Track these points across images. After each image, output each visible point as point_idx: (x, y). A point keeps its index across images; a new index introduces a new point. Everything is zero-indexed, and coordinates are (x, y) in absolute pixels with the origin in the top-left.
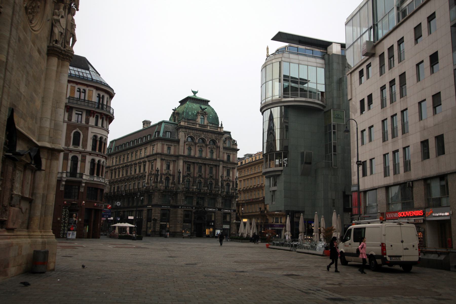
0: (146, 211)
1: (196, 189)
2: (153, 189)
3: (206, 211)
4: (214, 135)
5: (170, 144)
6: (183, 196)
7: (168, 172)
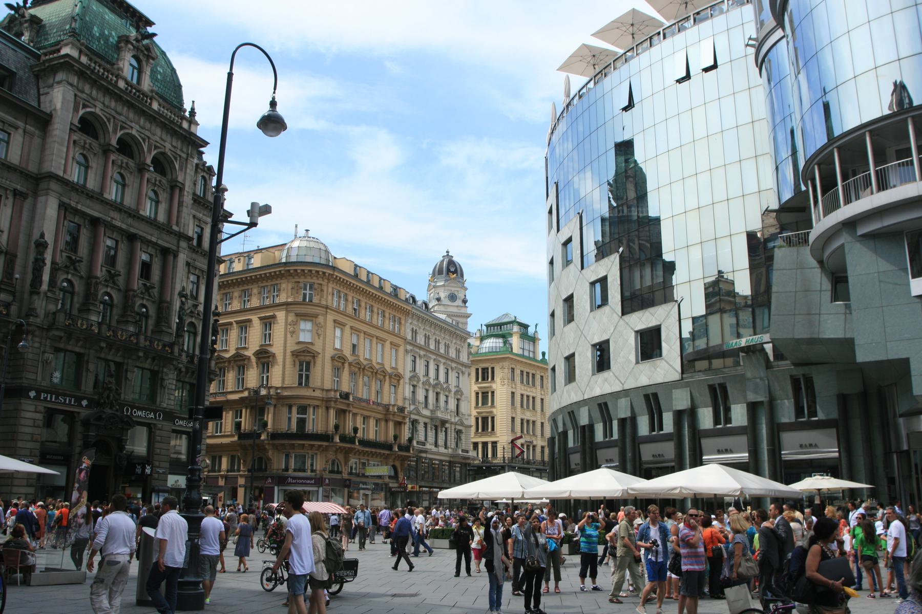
4: (168, 138)
6: (47, 349)
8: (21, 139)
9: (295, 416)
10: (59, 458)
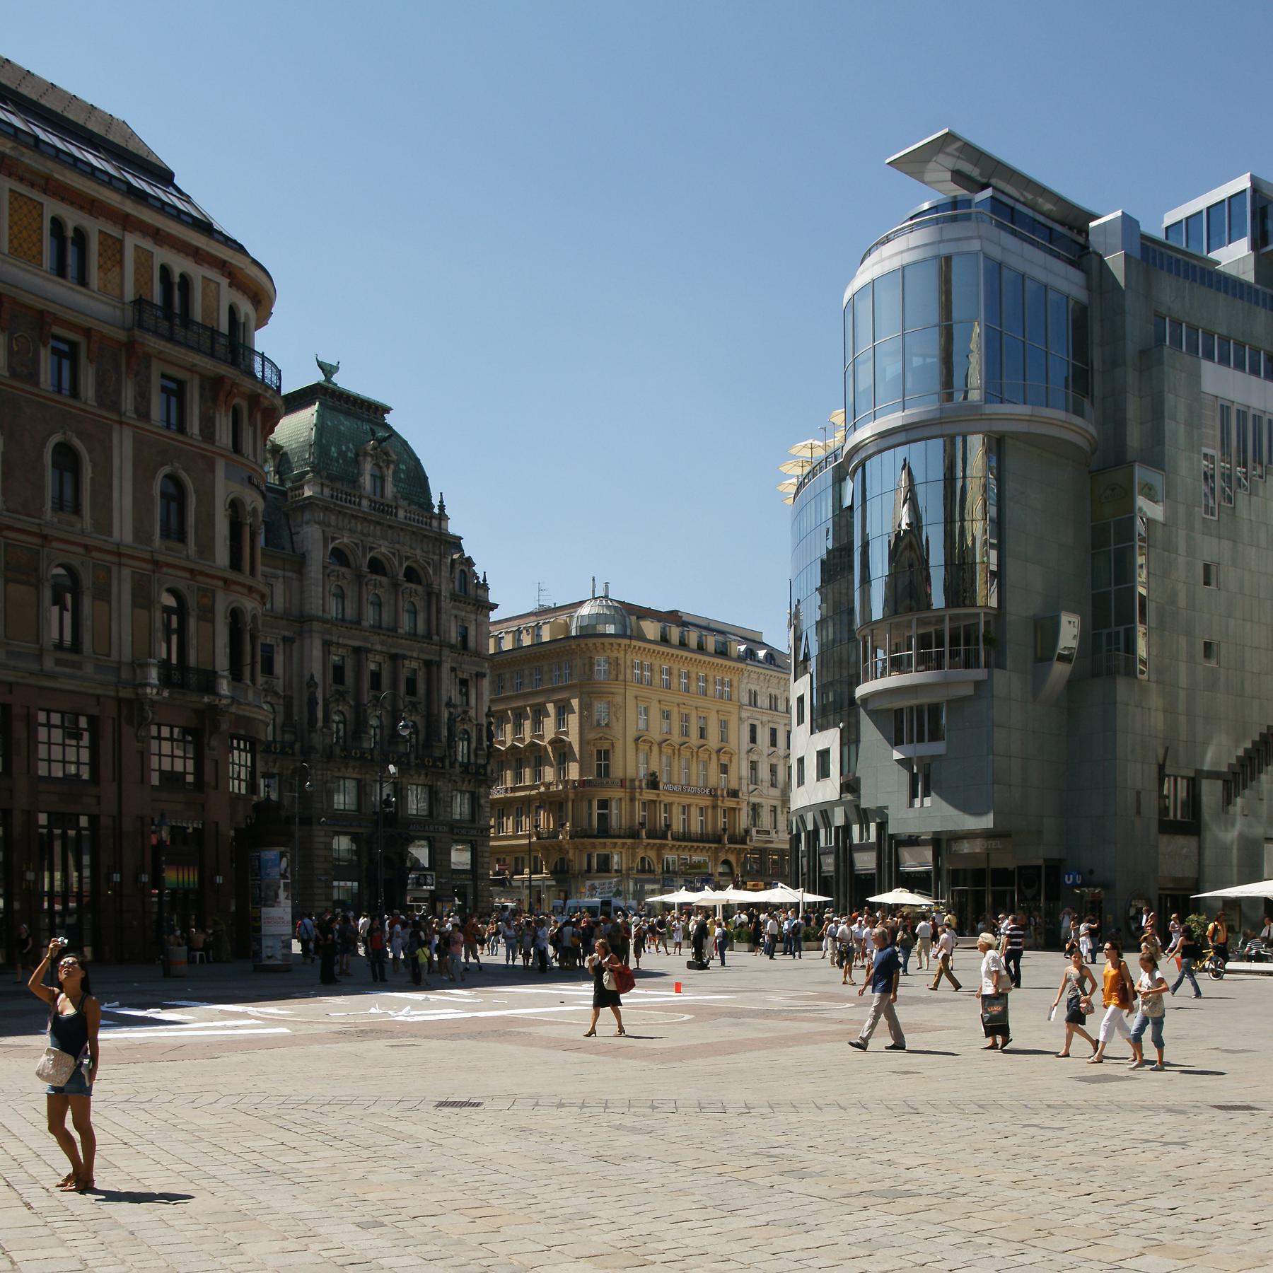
8: (282, 587)
9: (596, 811)
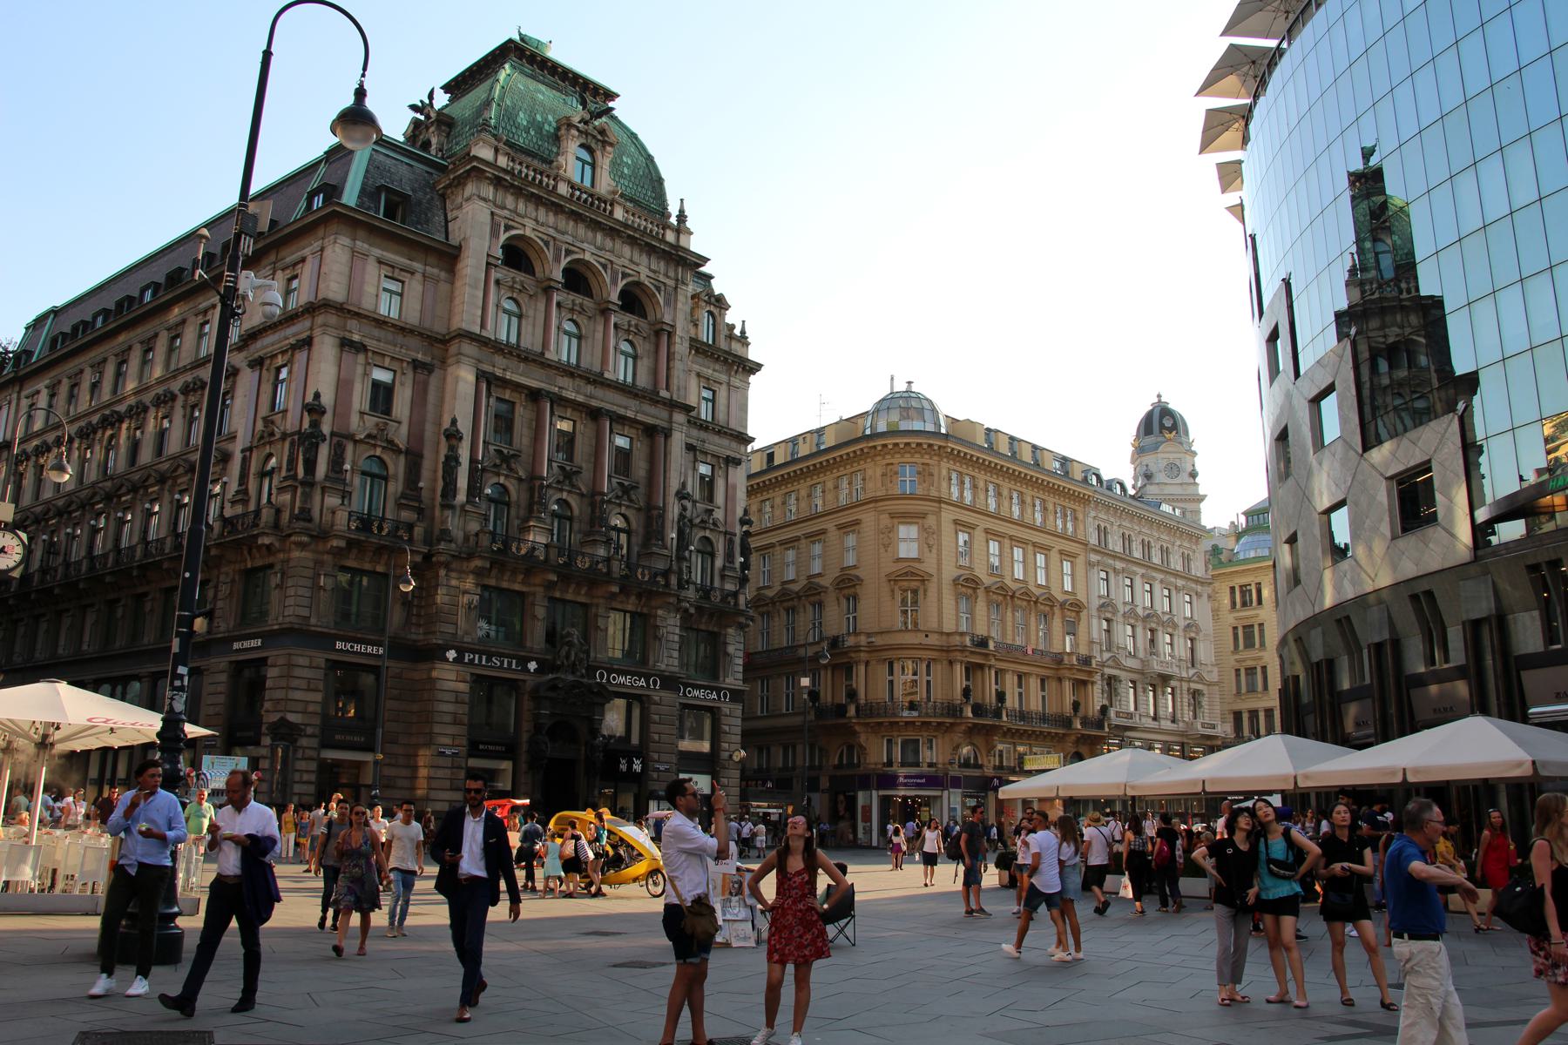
0: (223, 677)
1: (546, 546)
2: (276, 525)
3: (600, 684)
4: (644, 259)
5: (401, 260)
7: (382, 429)
8: (420, 288)
10: (498, 748)
